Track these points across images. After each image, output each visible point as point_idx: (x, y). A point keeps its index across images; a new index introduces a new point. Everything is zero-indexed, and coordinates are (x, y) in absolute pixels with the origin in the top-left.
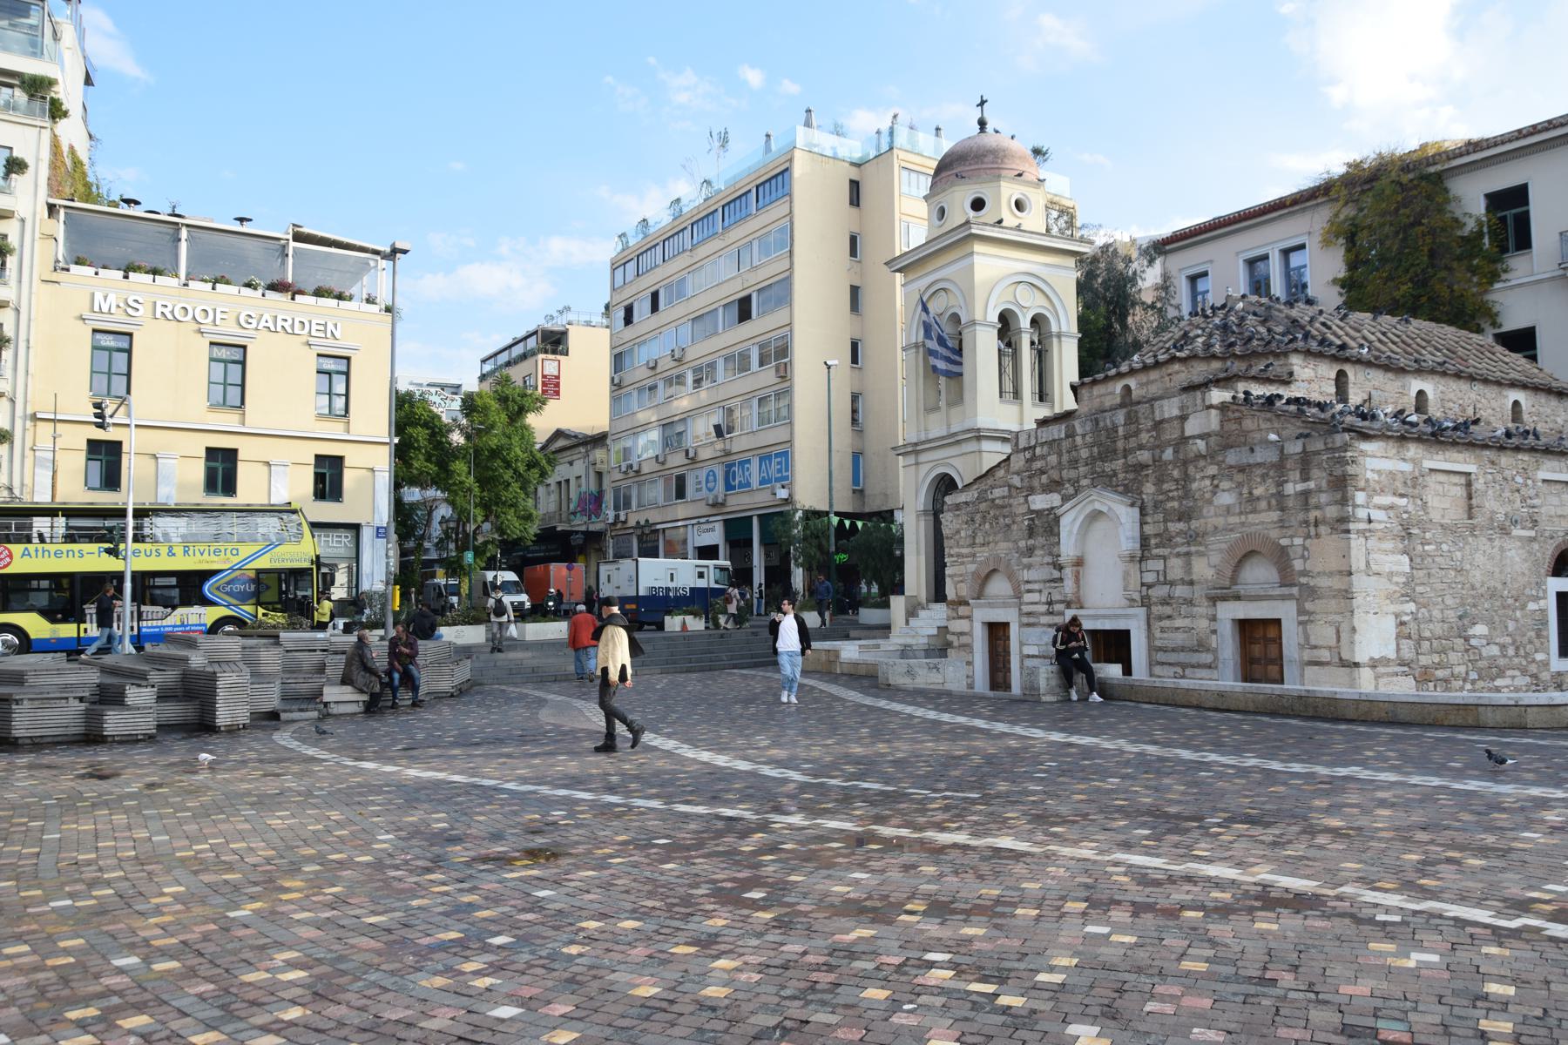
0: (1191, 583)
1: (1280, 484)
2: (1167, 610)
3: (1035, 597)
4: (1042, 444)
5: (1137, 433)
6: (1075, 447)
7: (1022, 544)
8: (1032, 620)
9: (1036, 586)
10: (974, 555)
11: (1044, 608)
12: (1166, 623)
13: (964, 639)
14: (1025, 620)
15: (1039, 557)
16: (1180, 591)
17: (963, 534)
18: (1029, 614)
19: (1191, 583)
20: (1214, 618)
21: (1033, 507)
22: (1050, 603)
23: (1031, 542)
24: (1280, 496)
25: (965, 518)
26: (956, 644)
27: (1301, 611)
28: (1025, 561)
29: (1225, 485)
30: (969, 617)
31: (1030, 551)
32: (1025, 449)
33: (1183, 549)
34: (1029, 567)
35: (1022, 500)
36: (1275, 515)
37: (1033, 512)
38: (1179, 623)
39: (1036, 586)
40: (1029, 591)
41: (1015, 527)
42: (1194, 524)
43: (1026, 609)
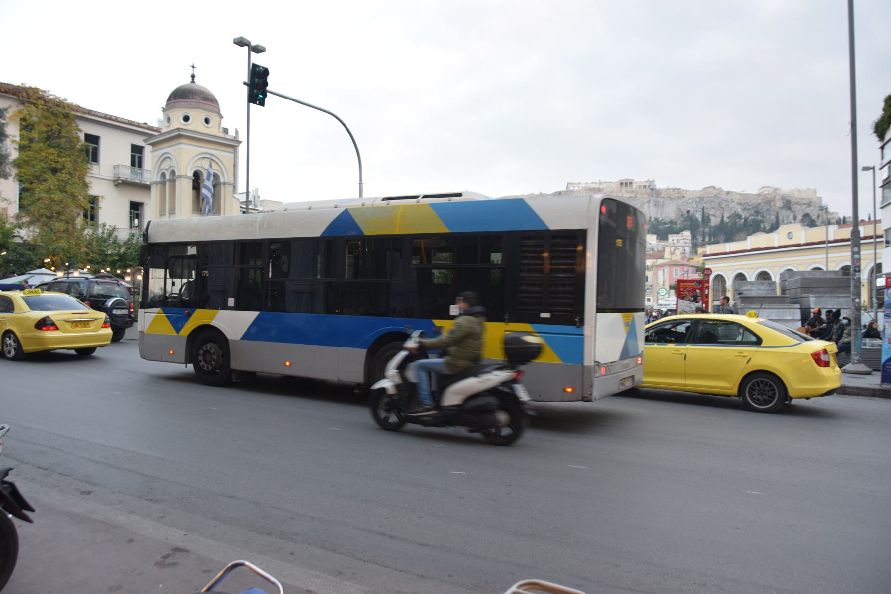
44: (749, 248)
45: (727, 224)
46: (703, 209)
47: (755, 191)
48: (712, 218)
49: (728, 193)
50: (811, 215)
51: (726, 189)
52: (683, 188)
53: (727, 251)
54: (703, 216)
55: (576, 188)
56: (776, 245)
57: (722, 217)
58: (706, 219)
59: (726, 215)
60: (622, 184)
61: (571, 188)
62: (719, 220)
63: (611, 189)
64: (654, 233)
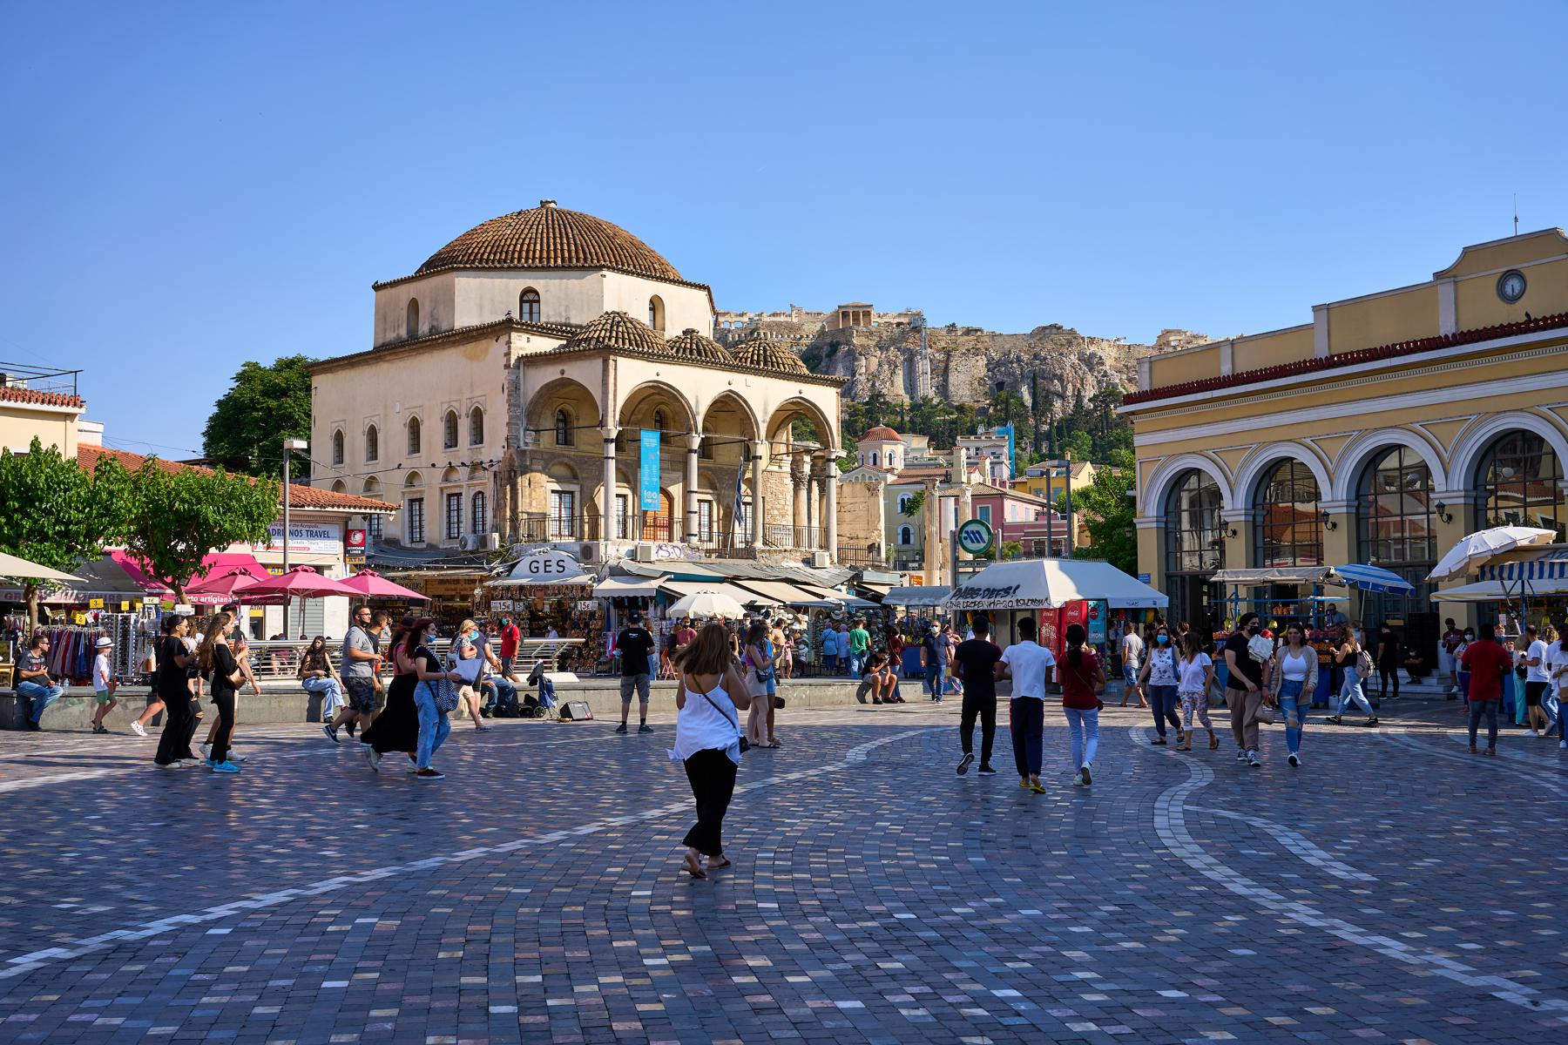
44: (1321, 352)
45: (1089, 413)
46: (1034, 380)
48: (1058, 404)
49: (1092, 340)
51: (1083, 332)
53: (1226, 370)
54: (1034, 395)
56: (1447, 328)
57: (1079, 398)
58: (1042, 402)
59: (1090, 392)
60: (845, 315)
61: (727, 326)
63: (818, 327)
64: (922, 432)
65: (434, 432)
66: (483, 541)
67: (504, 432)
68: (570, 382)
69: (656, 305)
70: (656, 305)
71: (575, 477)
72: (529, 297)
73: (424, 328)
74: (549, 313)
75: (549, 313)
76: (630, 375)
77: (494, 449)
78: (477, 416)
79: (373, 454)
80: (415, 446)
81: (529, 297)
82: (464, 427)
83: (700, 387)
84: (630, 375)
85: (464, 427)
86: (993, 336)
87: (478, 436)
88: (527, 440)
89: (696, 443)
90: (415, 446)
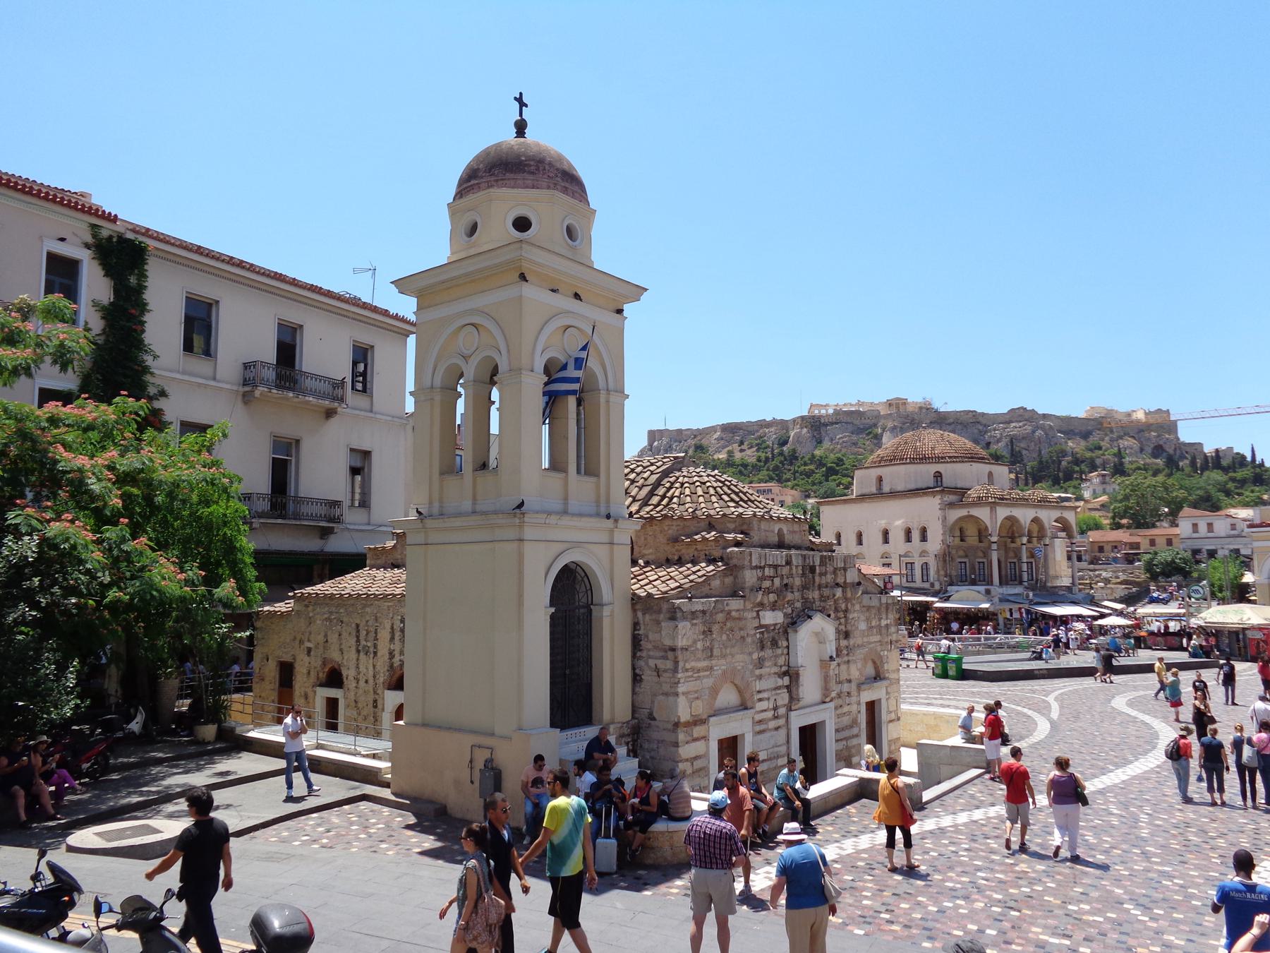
0: (850, 681)
1: (880, 619)
2: (840, 702)
3: (764, 705)
4: (770, 566)
5: (825, 574)
6: (791, 575)
7: (755, 656)
8: (763, 727)
9: (765, 695)
10: (711, 668)
11: (770, 714)
12: (840, 711)
13: (698, 764)
14: (758, 728)
15: (769, 669)
16: (846, 687)
17: (699, 645)
18: (760, 722)
19: (850, 681)
20: (859, 703)
21: (763, 622)
22: (775, 709)
23: (762, 654)
24: (879, 626)
25: (702, 628)
26: (689, 771)
27: (887, 693)
28: (758, 672)
29: (863, 618)
30: (705, 738)
31: (760, 663)
32: (756, 567)
33: (846, 659)
34: (760, 677)
35: (755, 614)
36: (877, 638)
37: (761, 626)
38: (846, 709)
39: (765, 695)
40: (760, 700)
41: (749, 640)
42: (852, 642)
43: (758, 717)
47: (1081, 414)
48: (1024, 452)
49: (1045, 416)
50: (1166, 447)
51: (1040, 412)
52: (979, 411)
55: (823, 412)
62: (1035, 455)
65: (897, 536)
66: (932, 585)
67: (941, 537)
68: (972, 516)
69: (990, 474)
70: (990, 474)
71: (966, 556)
72: (938, 475)
73: (886, 489)
74: (947, 481)
75: (947, 481)
76: (1002, 513)
77: (935, 544)
78: (924, 532)
79: (860, 542)
80: (886, 541)
81: (938, 475)
82: (916, 536)
83: (1025, 515)
84: (1002, 513)
85: (916, 536)
86: (983, 414)
87: (924, 538)
88: (949, 540)
89: (1025, 540)
90: (886, 541)
